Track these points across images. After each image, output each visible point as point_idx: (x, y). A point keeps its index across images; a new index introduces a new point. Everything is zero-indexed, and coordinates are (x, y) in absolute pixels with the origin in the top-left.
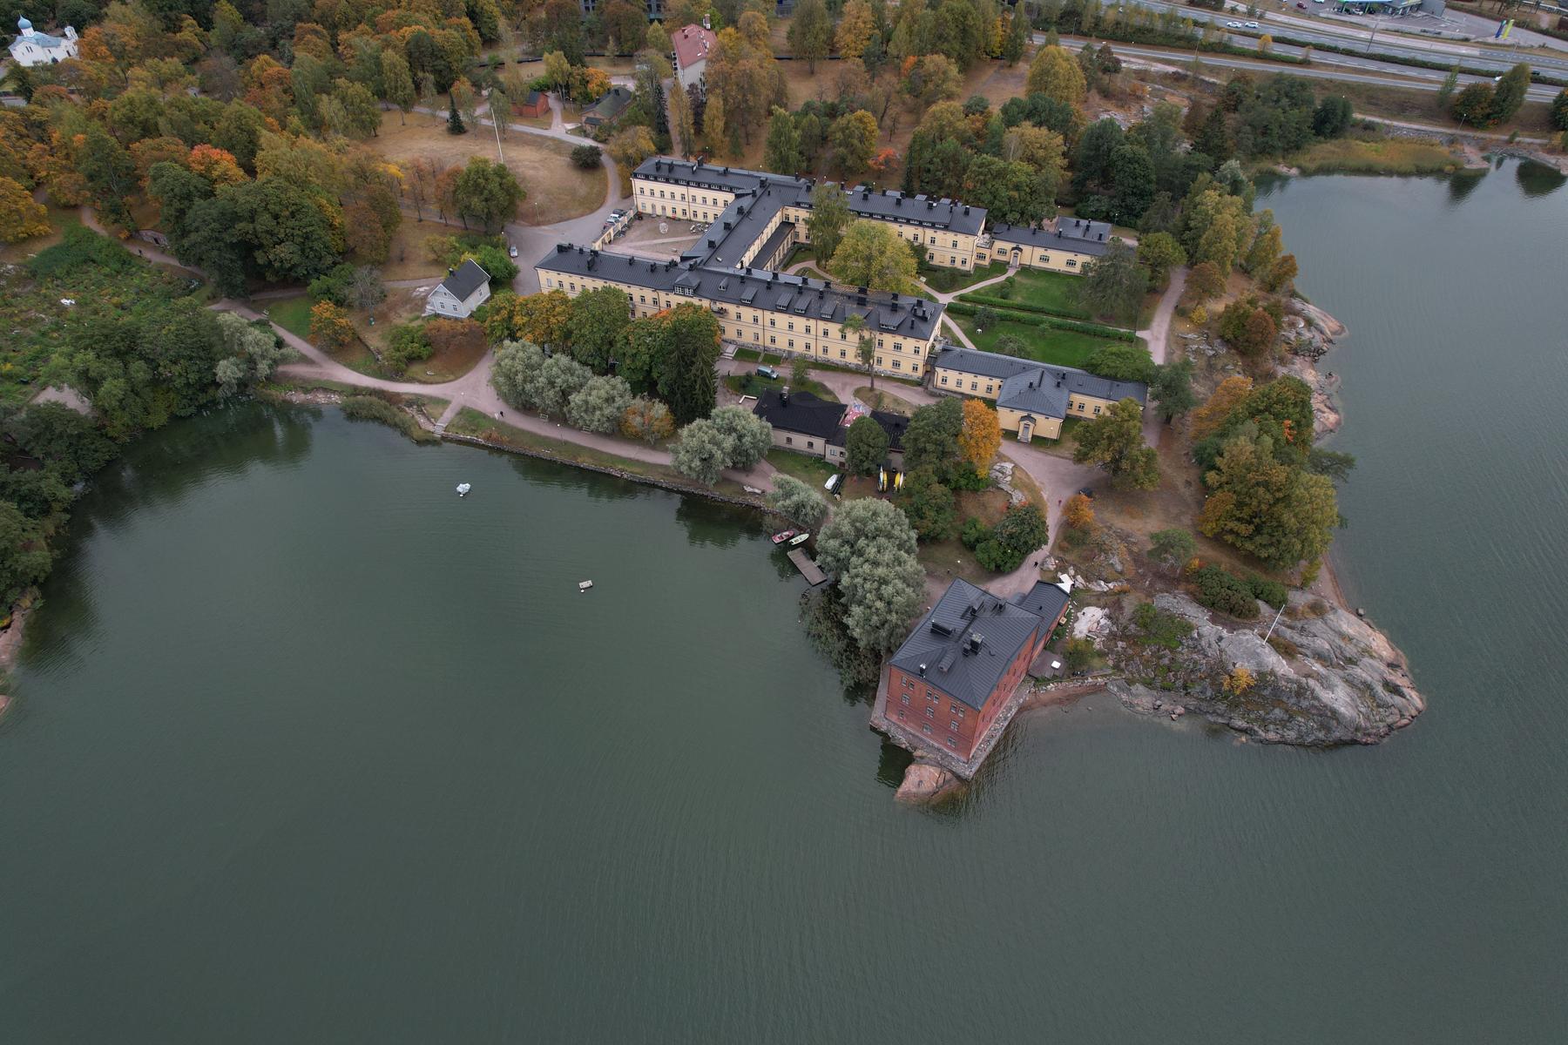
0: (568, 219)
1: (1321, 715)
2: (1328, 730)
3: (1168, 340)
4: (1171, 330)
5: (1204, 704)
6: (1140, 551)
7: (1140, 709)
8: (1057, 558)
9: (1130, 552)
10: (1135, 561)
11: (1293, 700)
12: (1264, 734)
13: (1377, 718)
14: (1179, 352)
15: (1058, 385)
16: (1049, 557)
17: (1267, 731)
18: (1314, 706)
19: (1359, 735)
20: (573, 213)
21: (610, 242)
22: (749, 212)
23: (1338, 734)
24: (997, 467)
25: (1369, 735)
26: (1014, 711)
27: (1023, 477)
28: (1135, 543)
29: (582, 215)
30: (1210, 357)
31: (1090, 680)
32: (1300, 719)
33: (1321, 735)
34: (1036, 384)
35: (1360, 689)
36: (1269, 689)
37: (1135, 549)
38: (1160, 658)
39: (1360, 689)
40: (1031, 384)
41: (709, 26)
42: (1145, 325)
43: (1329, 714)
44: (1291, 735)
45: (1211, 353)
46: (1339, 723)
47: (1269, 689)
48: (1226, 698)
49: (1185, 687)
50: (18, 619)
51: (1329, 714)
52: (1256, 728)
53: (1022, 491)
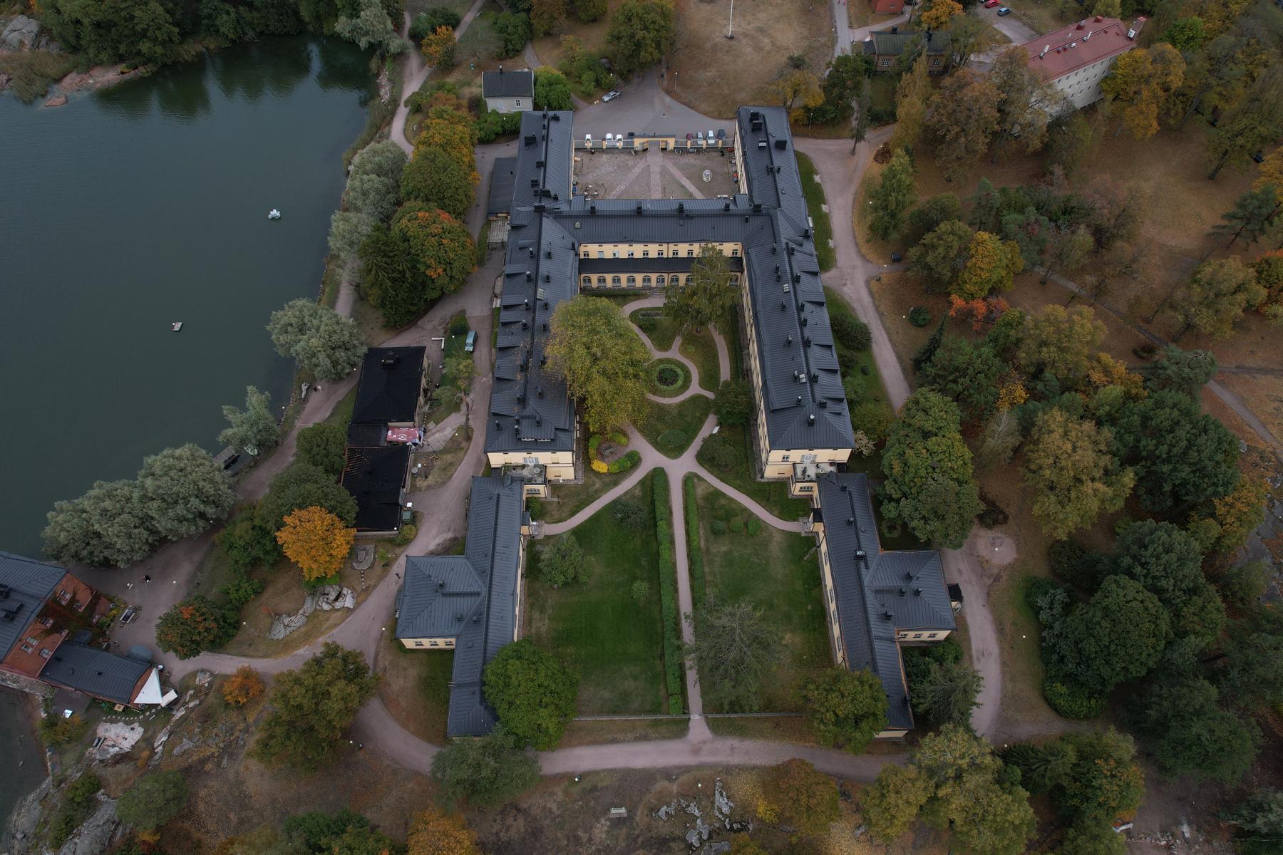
0: (692, 108)
3: (701, 767)
4: (728, 770)
6: (207, 773)
7: (15, 817)
8: (211, 684)
9: (203, 762)
10: (187, 770)
14: (675, 788)
15: (460, 620)
16: (212, 674)
20: (703, 106)
21: (664, 150)
22: (689, 217)
24: (345, 591)
26: (14, 686)
27: (331, 621)
28: (219, 765)
29: (705, 114)
30: (684, 840)
31: (49, 754)
34: (449, 590)
37: (208, 767)
40: (442, 586)
41: (1132, 33)
42: (717, 728)
45: (694, 840)
50: (131, 74)
53: (306, 624)
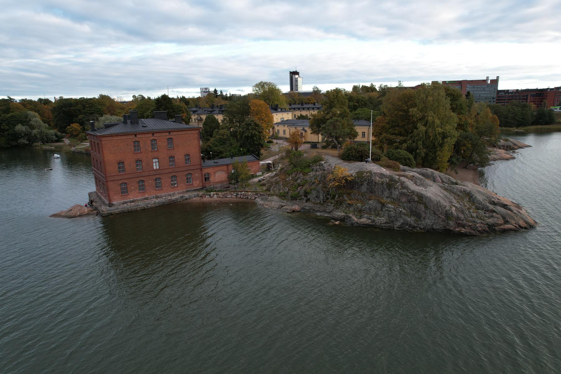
1: (409, 202)
2: (418, 216)
5: (319, 206)
11: (386, 193)
12: (356, 220)
13: (474, 215)
17: (361, 217)
18: (403, 194)
19: (451, 223)
23: (428, 222)
25: (463, 226)
32: (390, 205)
33: (411, 220)
35: (458, 196)
36: (365, 183)
38: (296, 181)
39: (458, 196)
43: (416, 199)
44: (381, 220)
46: (426, 207)
47: (365, 183)
48: (333, 197)
49: (306, 196)
51: (416, 199)
52: (351, 215)
